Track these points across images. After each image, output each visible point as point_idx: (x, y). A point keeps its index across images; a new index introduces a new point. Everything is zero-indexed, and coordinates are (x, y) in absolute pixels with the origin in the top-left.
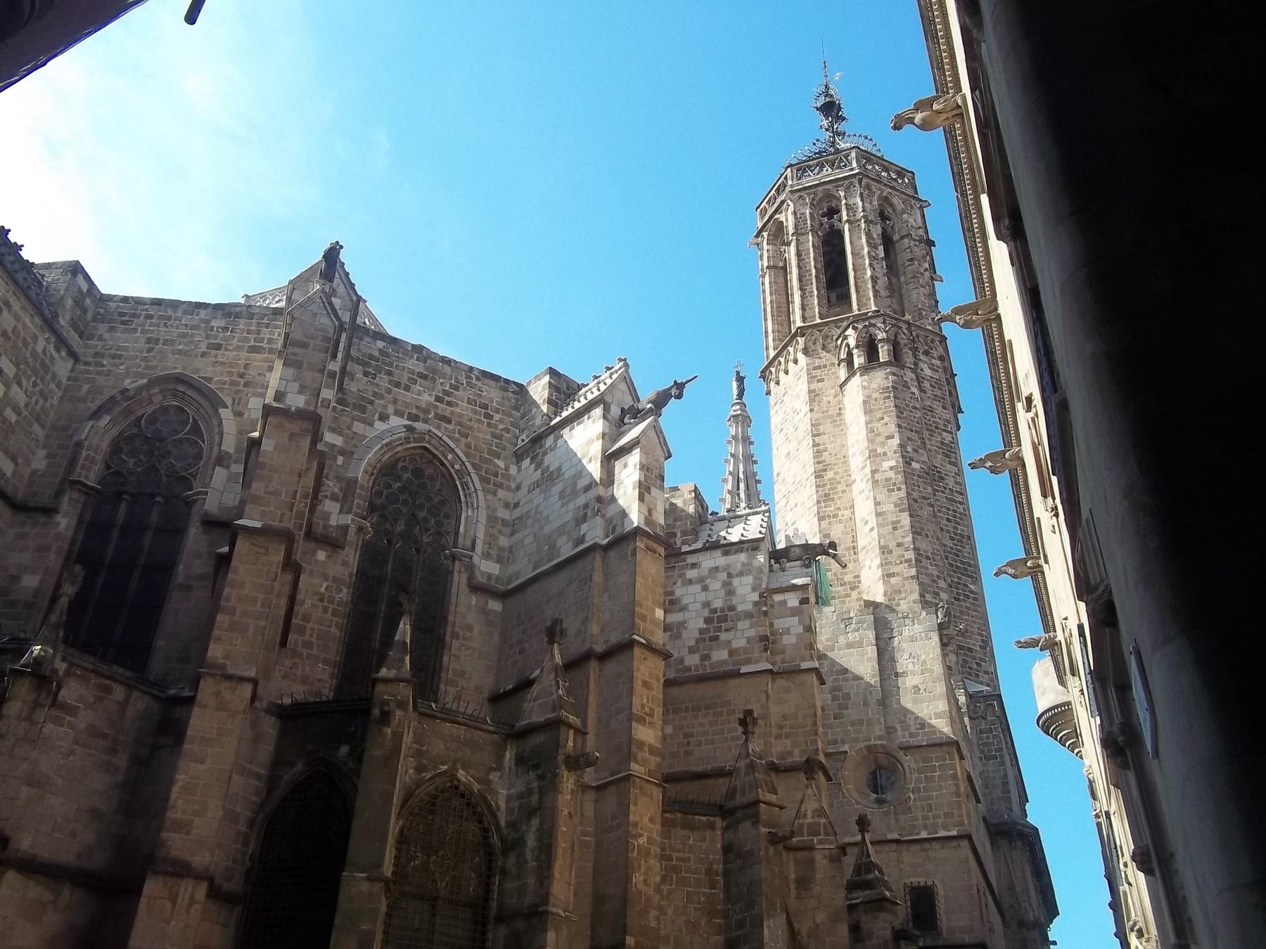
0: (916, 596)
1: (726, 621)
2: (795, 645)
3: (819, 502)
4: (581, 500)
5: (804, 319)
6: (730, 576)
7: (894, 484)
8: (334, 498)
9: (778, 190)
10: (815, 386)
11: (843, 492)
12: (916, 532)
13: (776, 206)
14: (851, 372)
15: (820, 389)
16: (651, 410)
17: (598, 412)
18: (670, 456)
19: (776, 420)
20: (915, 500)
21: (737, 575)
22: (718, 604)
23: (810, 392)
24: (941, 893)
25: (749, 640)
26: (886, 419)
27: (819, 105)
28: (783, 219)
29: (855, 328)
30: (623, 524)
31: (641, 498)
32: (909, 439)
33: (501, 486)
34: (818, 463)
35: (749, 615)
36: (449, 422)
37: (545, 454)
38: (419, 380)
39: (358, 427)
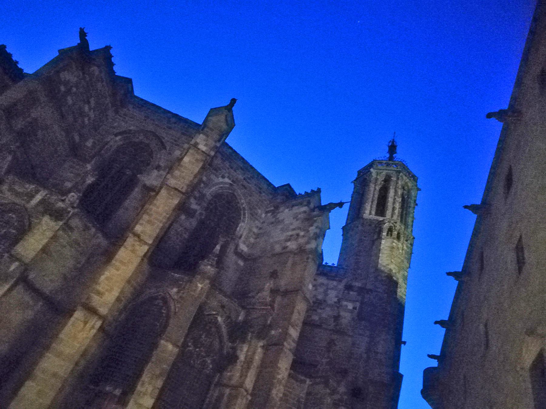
4: (290, 233)
8: (195, 198)
22: (320, 297)
33: (257, 220)
35: (331, 306)
36: (246, 188)
37: (279, 213)
38: (240, 170)
39: (213, 177)
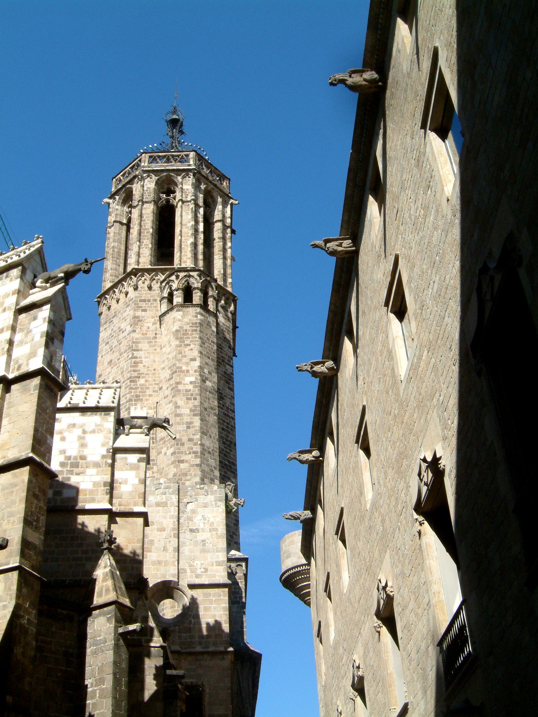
0: (198, 479)
1: (77, 466)
2: (130, 493)
3: (130, 400)
5: (138, 263)
6: (84, 432)
7: (192, 395)
9: (132, 168)
10: (139, 313)
11: (150, 395)
12: (204, 433)
13: (128, 179)
14: (171, 309)
15: (144, 317)
16: (62, 278)
17: (15, 272)
18: (71, 319)
19: (103, 335)
20: (206, 409)
21: (91, 432)
23: (135, 317)
24: (207, 691)
25: (95, 484)
26: (192, 346)
27: (168, 119)
28: (134, 189)
29: (177, 277)
30: (28, 364)
31: (47, 346)
32: (207, 364)
34: (134, 371)
35: (97, 465)
